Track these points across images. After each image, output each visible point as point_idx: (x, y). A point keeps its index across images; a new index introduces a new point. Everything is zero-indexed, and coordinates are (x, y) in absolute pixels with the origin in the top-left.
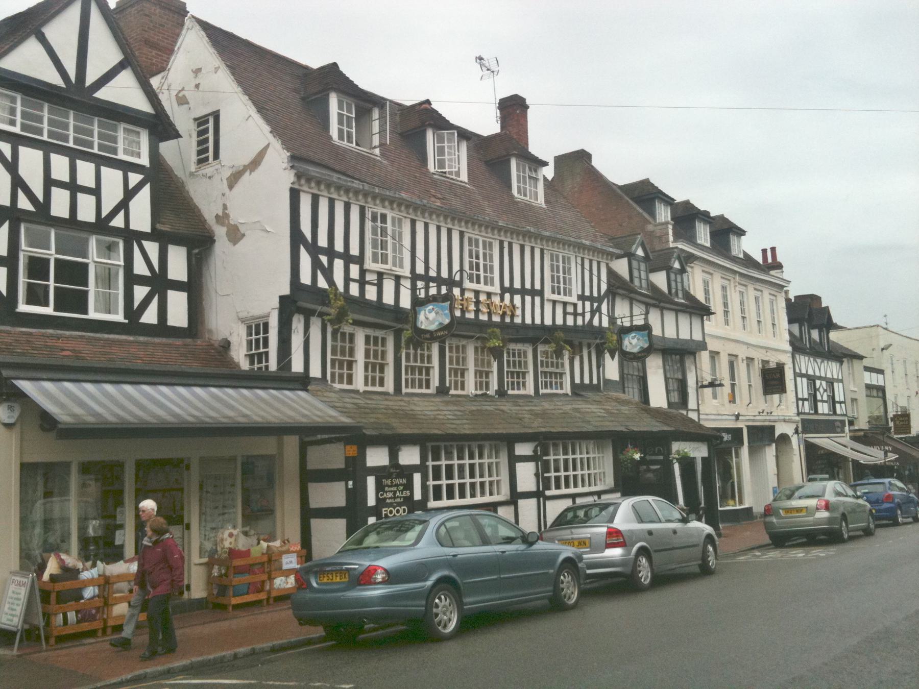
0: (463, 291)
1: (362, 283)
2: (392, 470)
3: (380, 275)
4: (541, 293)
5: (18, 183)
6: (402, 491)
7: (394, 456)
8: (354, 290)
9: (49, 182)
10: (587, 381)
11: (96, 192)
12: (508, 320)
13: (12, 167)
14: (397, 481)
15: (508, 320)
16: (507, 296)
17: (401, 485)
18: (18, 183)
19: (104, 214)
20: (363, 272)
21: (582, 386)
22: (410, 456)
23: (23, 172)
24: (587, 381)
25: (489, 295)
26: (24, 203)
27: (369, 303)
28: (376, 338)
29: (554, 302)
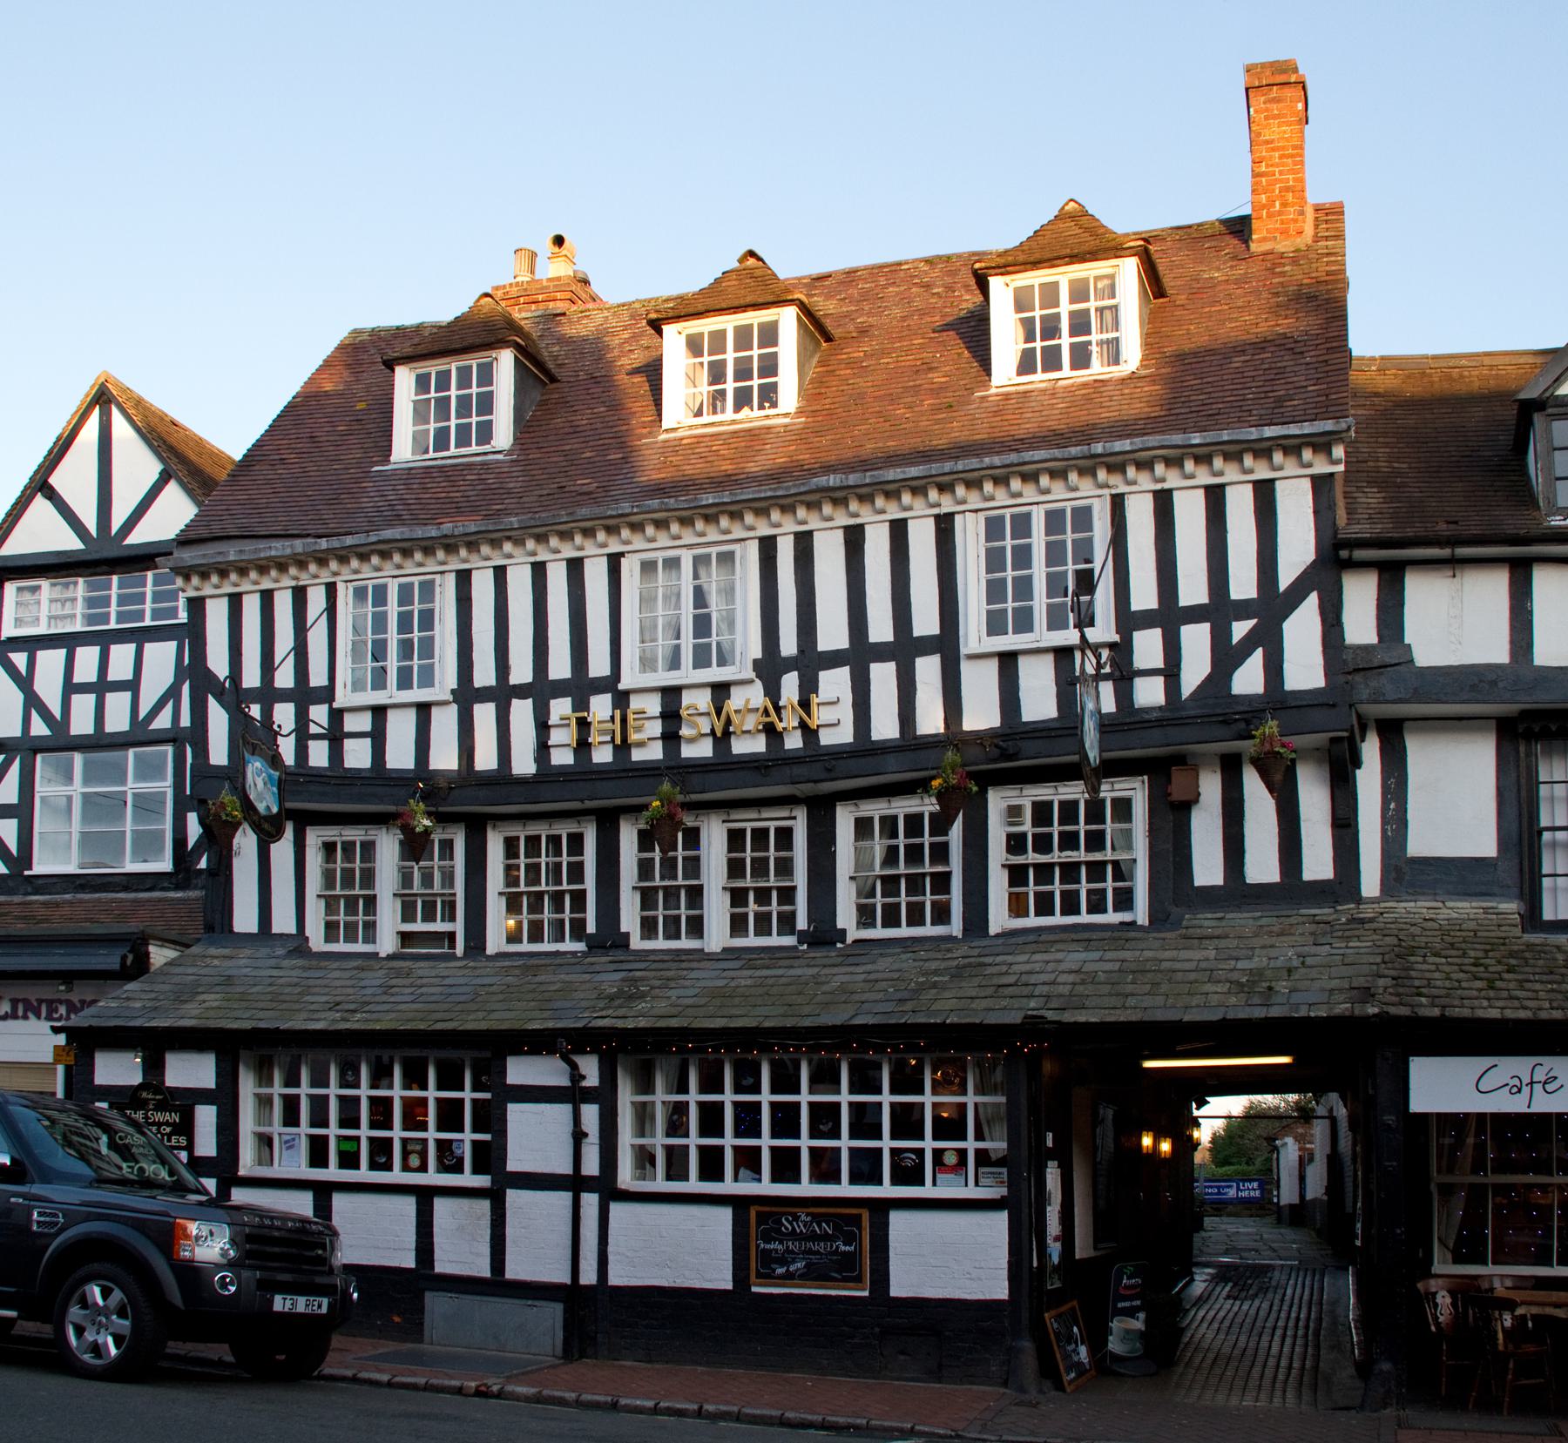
0: (621, 699)
1: (336, 736)
2: (144, 1095)
3: (379, 712)
4: (946, 644)
5: (33, 702)
6: (169, 1136)
7: (154, 1067)
8: (319, 755)
9: (71, 688)
10: (1262, 866)
11: (133, 686)
12: (794, 742)
13: (25, 682)
14: (159, 1117)
15: (794, 742)
16: (790, 685)
17: (167, 1124)
18: (33, 702)
19: (142, 714)
20: (337, 716)
21: (1237, 889)
22: (190, 1071)
23: (39, 687)
24: (1262, 866)
25: (721, 691)
26: (39, 728)
27: (356, 776)
28: (348, 847)
29: (1008, 660)
